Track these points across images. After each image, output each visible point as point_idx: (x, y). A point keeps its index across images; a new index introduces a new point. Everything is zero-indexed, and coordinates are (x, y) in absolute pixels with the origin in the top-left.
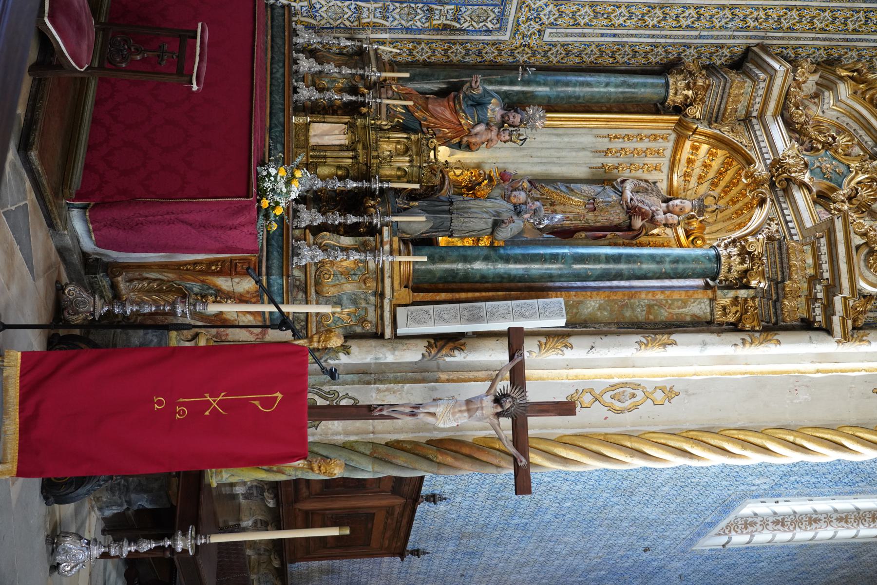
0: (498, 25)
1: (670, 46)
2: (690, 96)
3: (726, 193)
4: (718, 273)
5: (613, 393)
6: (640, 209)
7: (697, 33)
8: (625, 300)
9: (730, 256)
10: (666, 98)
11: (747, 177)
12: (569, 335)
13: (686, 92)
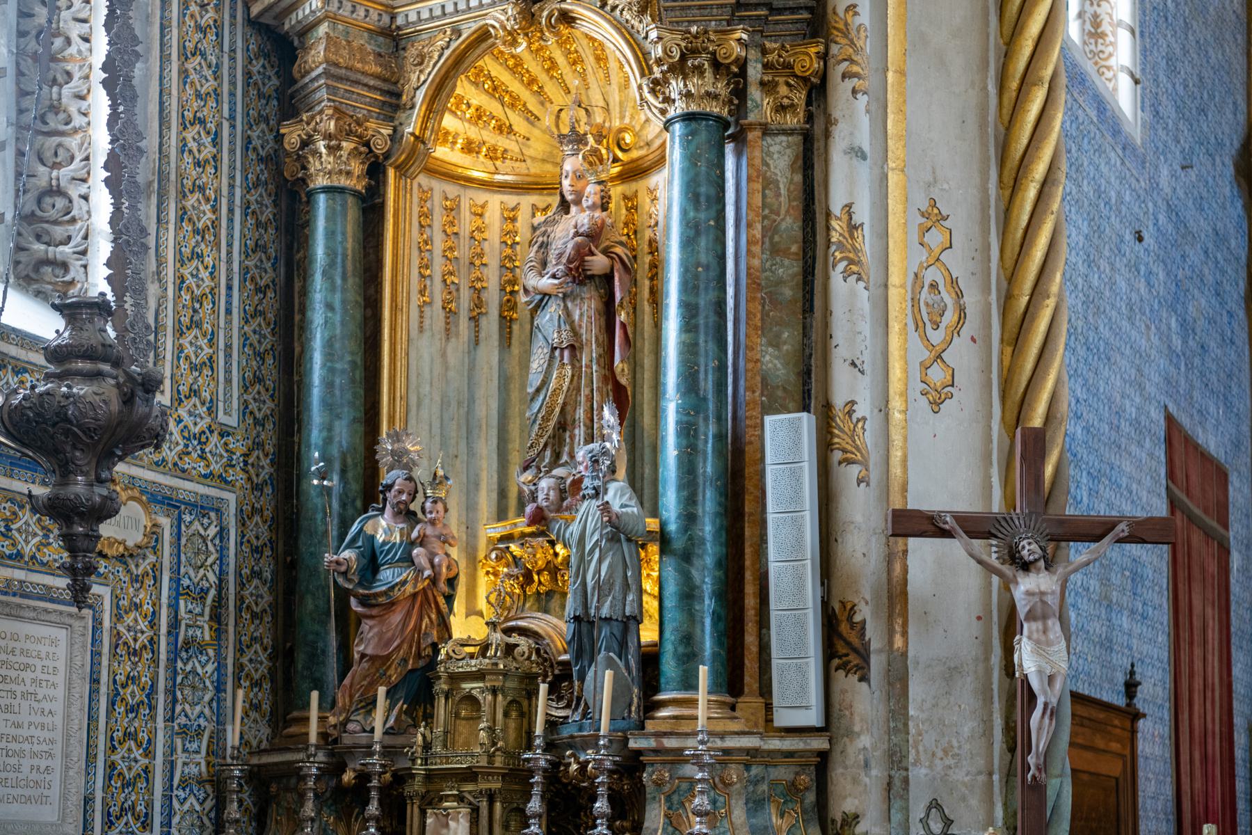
0: (213, 515)
1: (247, 179)
2: (352, 145)
3: (532, 81)
4: (718, 119)
5: (928, 325)
7: (226, 125)
8: (763, 298)
9: (688, 95)
10: (356, 194)
11: (514, 43)
12: (828, 406)
13: (344, 154)
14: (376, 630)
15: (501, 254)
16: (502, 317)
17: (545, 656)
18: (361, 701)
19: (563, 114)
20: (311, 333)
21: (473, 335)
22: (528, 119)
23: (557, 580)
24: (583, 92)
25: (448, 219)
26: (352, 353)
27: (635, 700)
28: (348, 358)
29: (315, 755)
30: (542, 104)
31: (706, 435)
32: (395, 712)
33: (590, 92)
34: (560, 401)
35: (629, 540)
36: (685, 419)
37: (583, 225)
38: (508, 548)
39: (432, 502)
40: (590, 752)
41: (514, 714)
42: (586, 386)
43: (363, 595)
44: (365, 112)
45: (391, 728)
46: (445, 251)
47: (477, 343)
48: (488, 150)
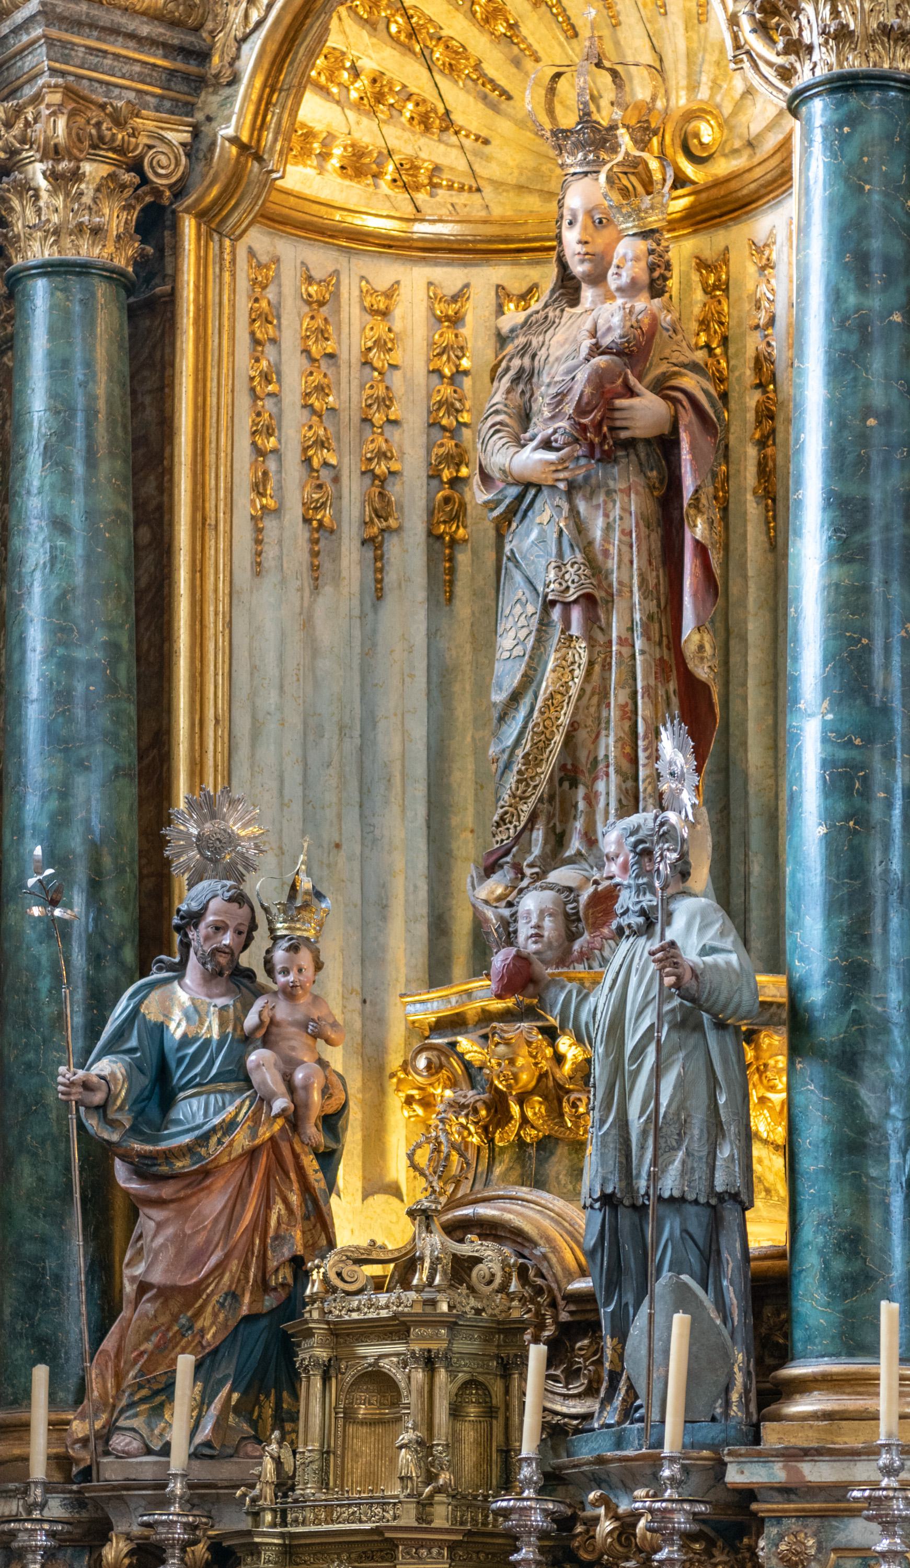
2: (104, 170)
10: (112, 275)
13: (87, 188)
14: (169, 1231)
15: (429, 397)
16: (433, 537)
17: (539, 1281)
18: (140, 1386)
19: (563, 85)
20: (21, 584)
21: (371, 576)
22: (485, 98)
24: (606, 32)
25: (314, 324)
26: (110, 626)
27: (739, 1378)
28: (102, 636)
29: (43, 1506)
30: (517, 63)
31: (889, 790)
32: (214, 1410)
33: (623, 34)
34: (564, 720)
35: (720, 1025)
36: (842, 754)
37: (609, 329)
38: (453, 1045)
39: (288, 950)
40: (640, 1492)
41: (472, 1411)
42: (620, 685)
43: (143, 1156)
44: (132, 95)
45: (207, 1444)
46: (308, 395)
47: (379, 594)
48: (399, 168)
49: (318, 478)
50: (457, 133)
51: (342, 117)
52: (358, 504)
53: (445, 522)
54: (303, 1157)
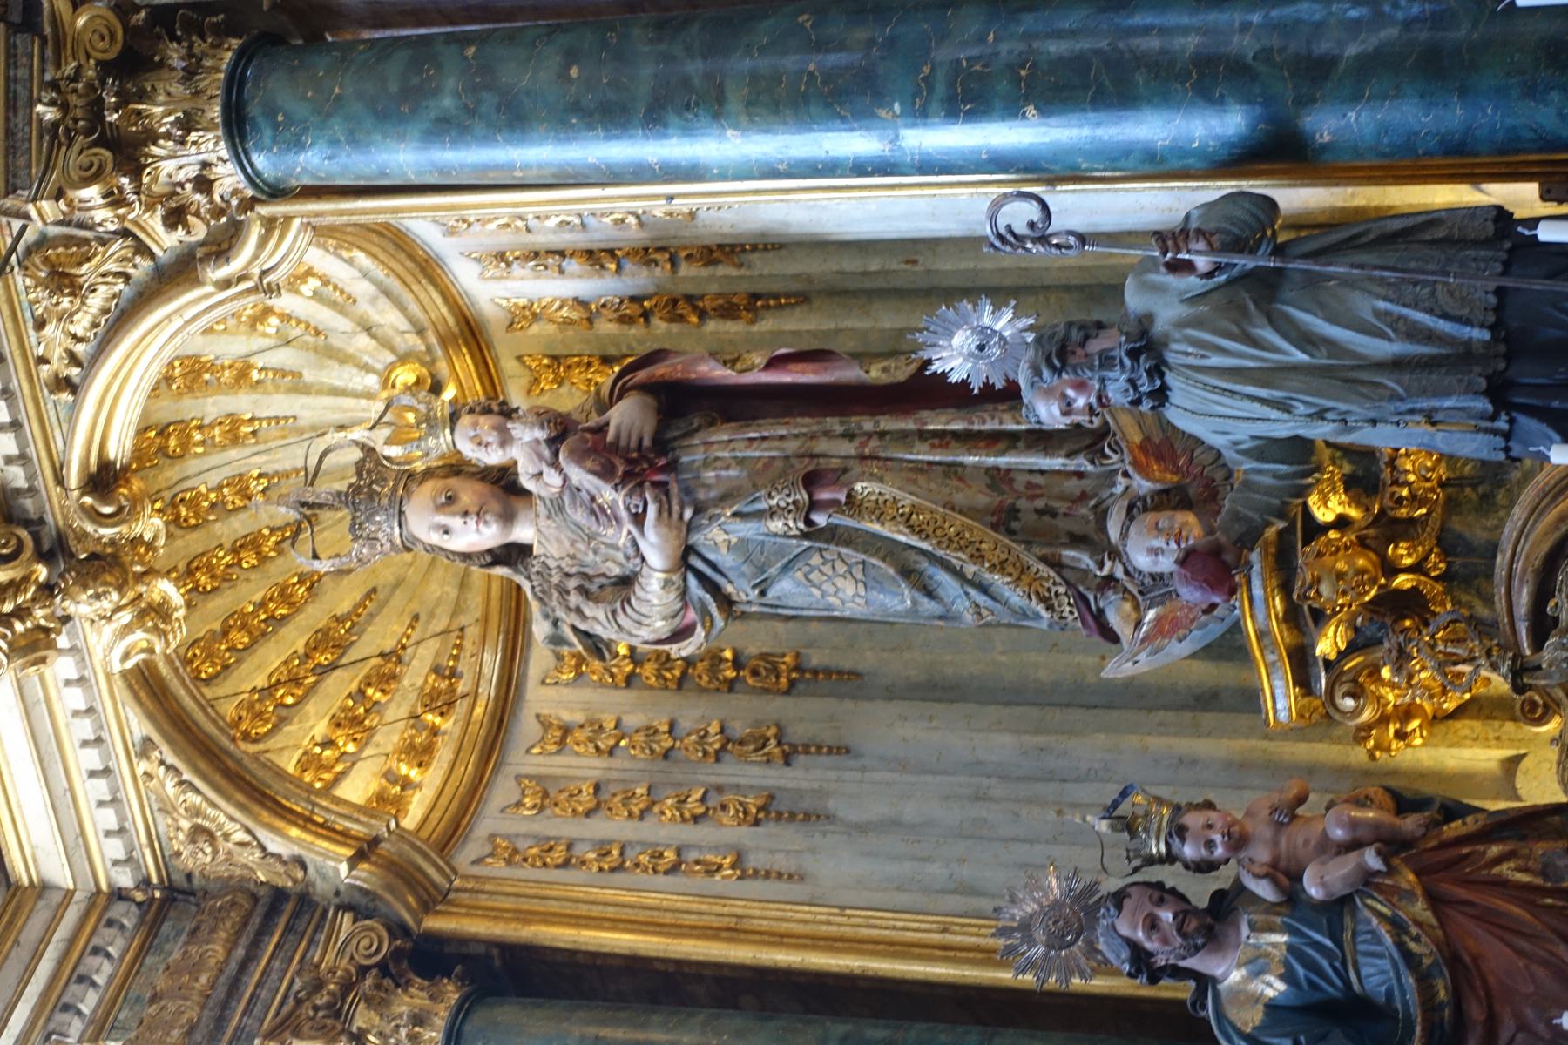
6: (605, 473)
15: (651, 688)
23: (1411, 521)
38: (1328, 664)
48: (428, 708)
49: (715, 809)
50: (404, 647)
51: (369, 762)
52: (747, 767)
53: (778, 677)
54: (1444, 837)
